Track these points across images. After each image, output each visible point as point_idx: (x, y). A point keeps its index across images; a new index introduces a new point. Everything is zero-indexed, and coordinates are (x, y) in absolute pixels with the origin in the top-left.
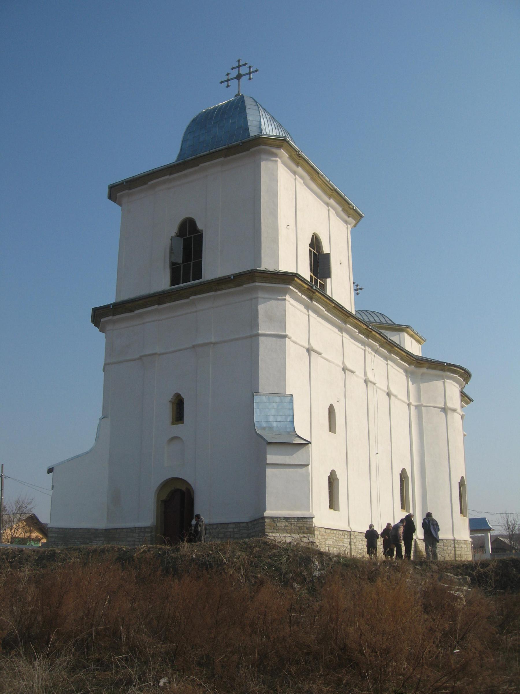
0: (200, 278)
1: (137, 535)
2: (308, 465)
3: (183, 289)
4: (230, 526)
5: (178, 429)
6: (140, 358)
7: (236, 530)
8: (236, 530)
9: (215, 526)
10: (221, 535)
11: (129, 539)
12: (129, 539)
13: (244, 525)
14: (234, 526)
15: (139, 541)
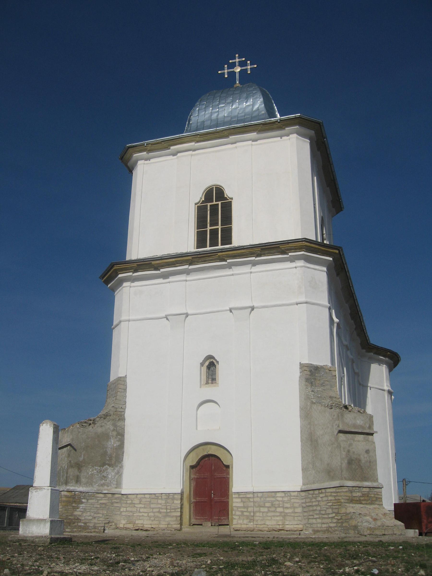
0: (231, 244)
1: (163, 502)
2: (372, 434)
3: (222, 251)
4: (278, 495)
5: (209, 392)
6: (166, 317)
7: (286, 499)
8: (286, 499)
9: (260, 495)
10: (268, 505)
11: (152, 506)
12: (152, 506)
13: (296, 494)
14: (283, 495)
15: (167, 509)
